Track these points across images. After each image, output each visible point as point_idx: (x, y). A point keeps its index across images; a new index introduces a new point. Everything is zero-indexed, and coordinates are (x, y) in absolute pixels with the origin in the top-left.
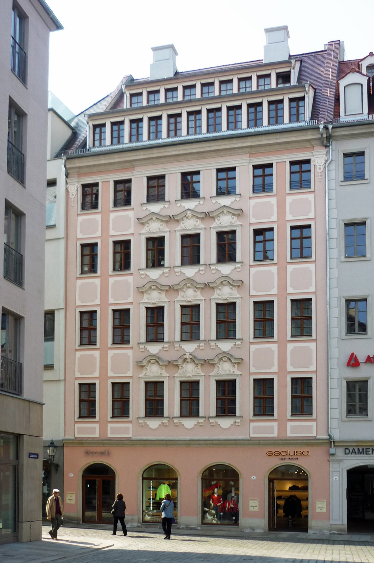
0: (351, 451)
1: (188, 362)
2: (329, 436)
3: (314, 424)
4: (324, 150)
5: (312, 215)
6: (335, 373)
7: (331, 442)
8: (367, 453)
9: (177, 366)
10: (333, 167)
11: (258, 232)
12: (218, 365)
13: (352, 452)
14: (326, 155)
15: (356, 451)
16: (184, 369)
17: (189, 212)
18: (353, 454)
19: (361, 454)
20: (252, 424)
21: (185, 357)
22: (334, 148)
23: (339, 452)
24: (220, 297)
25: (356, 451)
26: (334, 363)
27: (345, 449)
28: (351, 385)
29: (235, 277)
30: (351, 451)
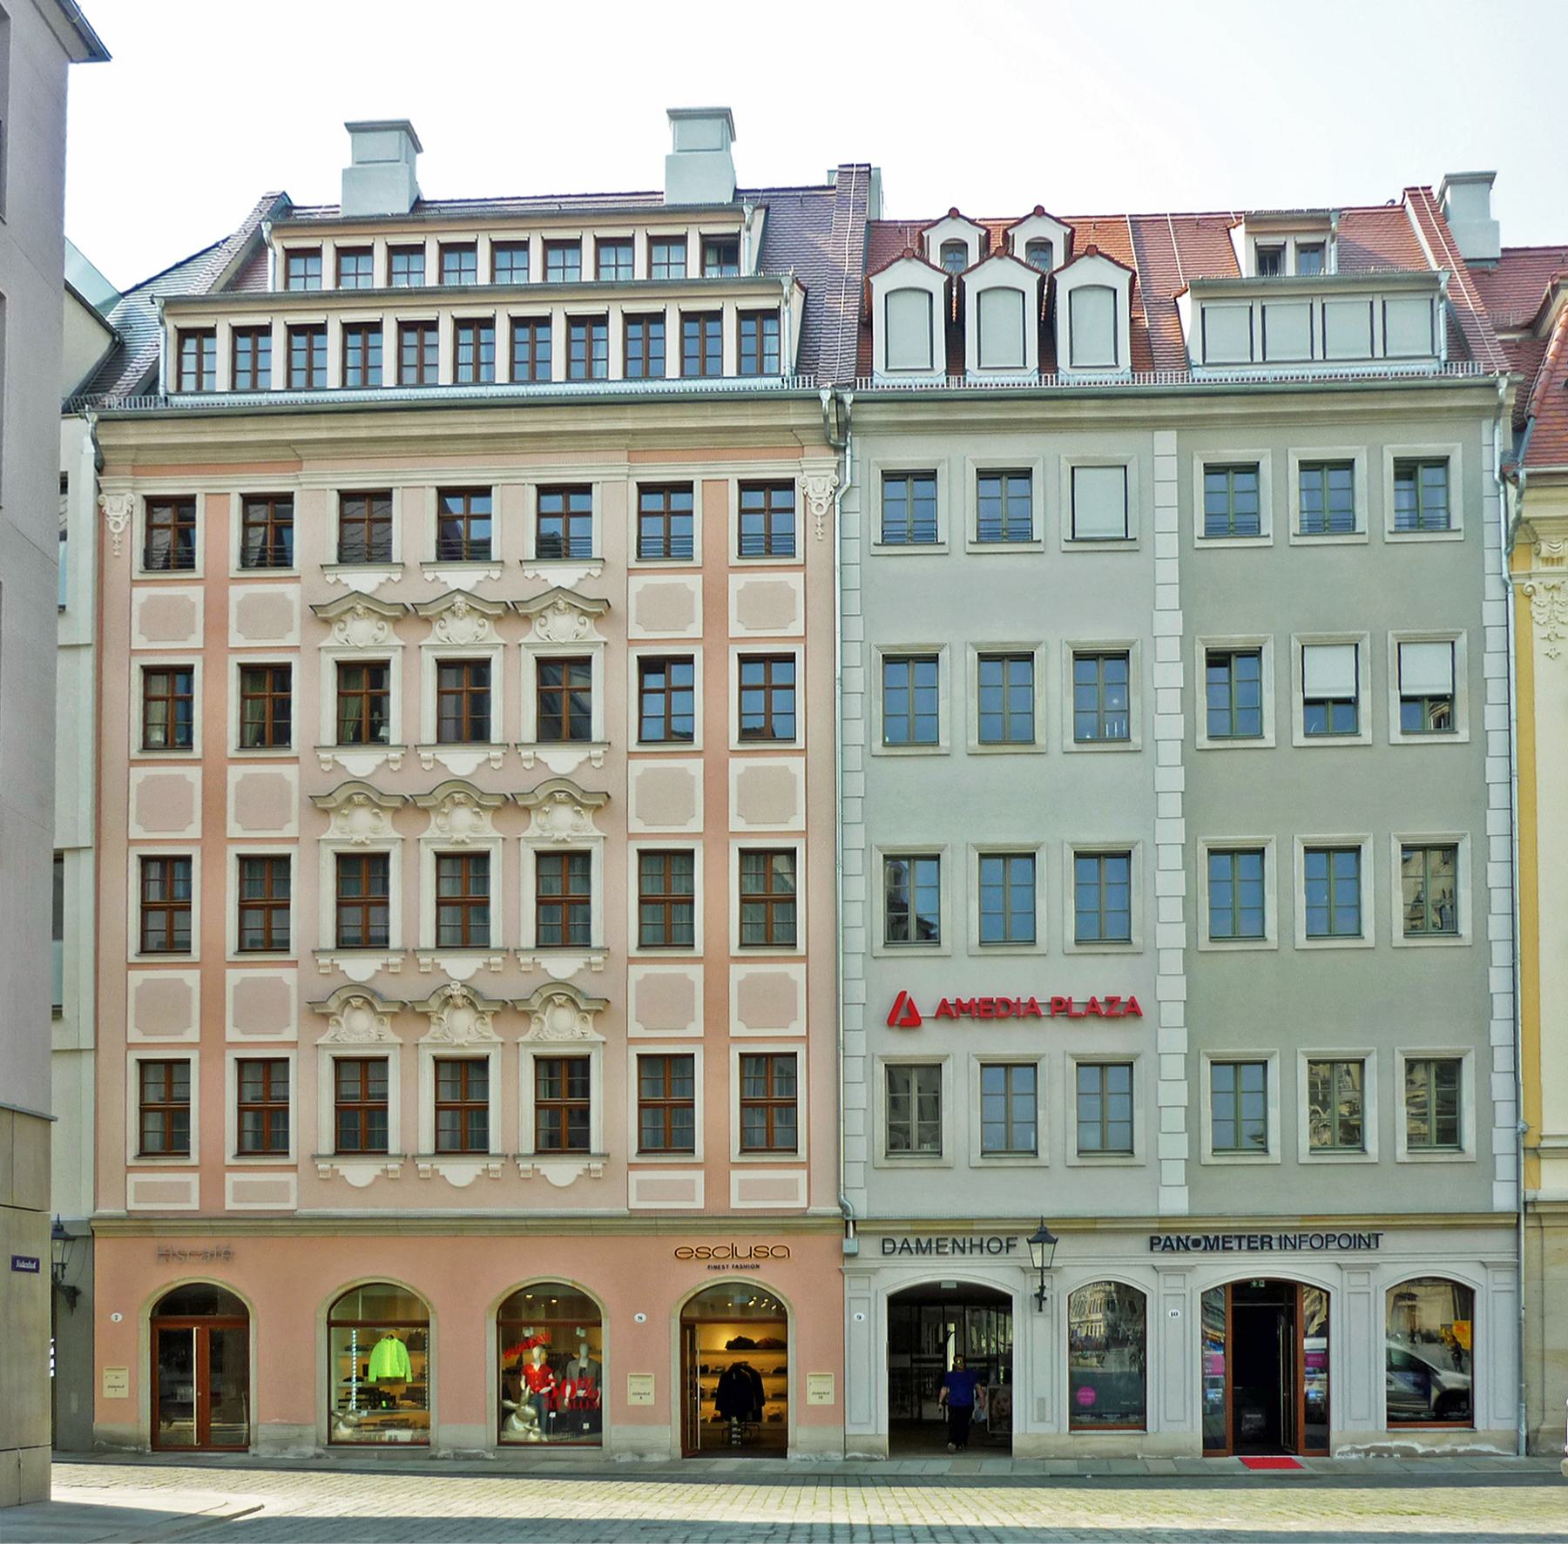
0: (899, 1246)
1: (456, 1007)
2: (842, 1206)
3: (801, 1175)
4: (831, 459)
5: (797, 629)
6: (857, 1044)
7: (846, 1223)
8: (940, 1250)
9: (426, 1016)
10: (854, 503)
11: (649, 665)
12: (540, 1015)
13: (902, 1248)
14: (837, 472)
15: (913, 1246)
16: (445, 1024)
17: (459, 598)
18: (905, 1254)
19: (924, 1253)
20: (635, 1176)
21: (448, 992)
22: (857, 457)
23: (868, 1248)
24: (545, 835)
25: (913, 1246)
26: (855, 1016)
27: (884, 1240)
28: (897, 1075)
29: (588, 782)
30: (899, 1246)
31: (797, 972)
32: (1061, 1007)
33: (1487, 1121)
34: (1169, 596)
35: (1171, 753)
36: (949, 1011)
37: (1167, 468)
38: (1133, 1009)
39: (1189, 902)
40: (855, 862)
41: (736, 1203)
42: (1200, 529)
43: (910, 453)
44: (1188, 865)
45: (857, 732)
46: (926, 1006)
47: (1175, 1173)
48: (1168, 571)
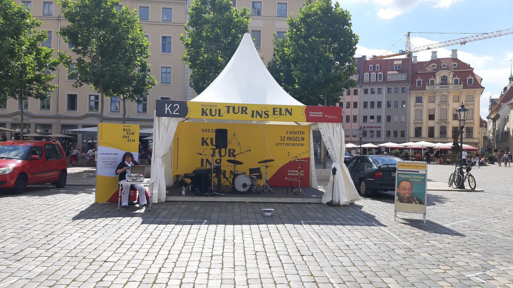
10: (362, 91)
31: (357, 124)
32: (375, 127)
33: (406, 136)
34: (384, 98)
35: (384, 109)
36: (368, 127)
37: (385, 88)
38: (381, 127)
39: (385, 119)
40: (361, 116)
41: (352, 140)
42: (387, 93)
43: (366, 88)
44: (385, 117)
45: (361, 107)
46: (366, 127)
47: (383, 138)
48: (384, 96)
